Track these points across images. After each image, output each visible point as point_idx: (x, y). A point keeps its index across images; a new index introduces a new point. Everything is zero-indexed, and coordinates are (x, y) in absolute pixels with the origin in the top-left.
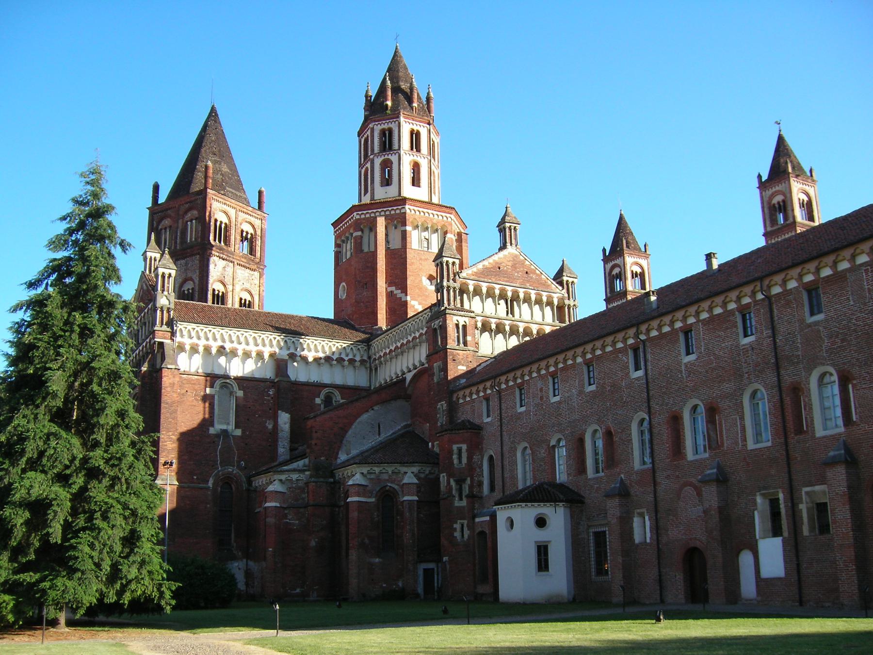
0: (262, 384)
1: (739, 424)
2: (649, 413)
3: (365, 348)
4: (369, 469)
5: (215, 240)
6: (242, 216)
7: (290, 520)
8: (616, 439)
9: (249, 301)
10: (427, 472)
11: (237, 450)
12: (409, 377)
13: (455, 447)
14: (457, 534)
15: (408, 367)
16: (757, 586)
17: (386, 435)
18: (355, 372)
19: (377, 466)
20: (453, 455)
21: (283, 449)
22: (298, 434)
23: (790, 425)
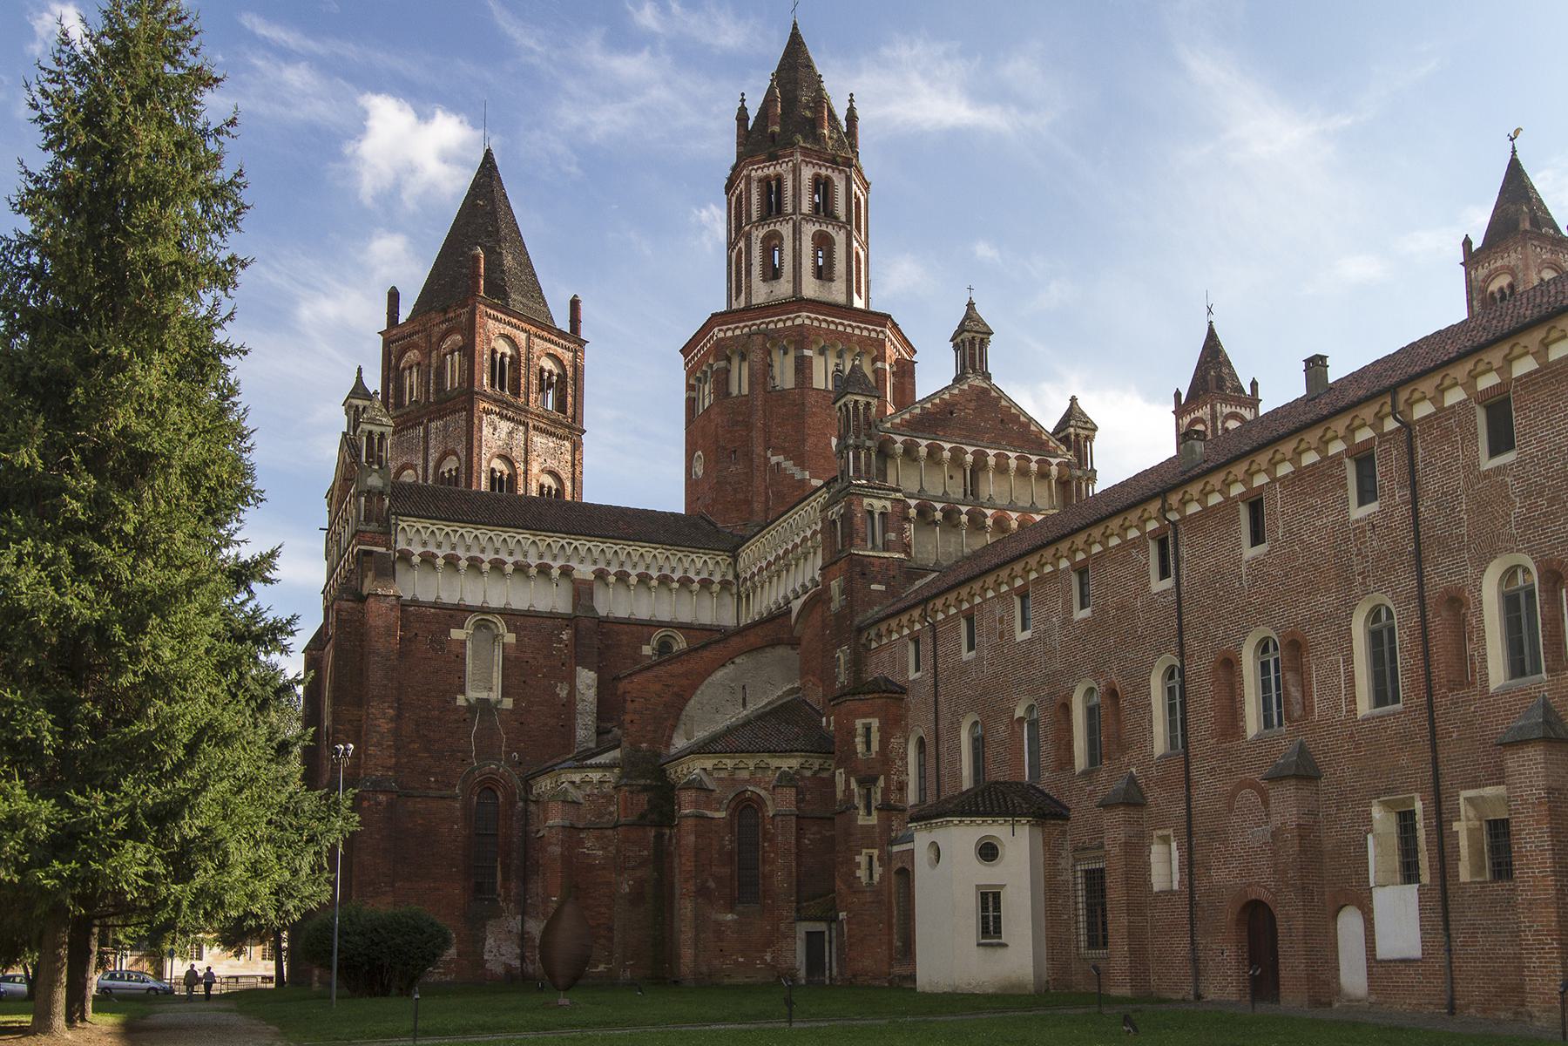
0: (549, 622)
1: (1342, 671)
2: (1182, 655)
3: (730, 560)
4: (716, 761)
5: (493, 386)
6: (539, 345)
10: (816, 767)
12: (796, 605)
14: (862, 873)
15: (794, 591)
16: (1370, 974)
17: (757, 704)
19: (729, 758)
21: (584, 731)
22: (608, 707)
23: (1440, 673)
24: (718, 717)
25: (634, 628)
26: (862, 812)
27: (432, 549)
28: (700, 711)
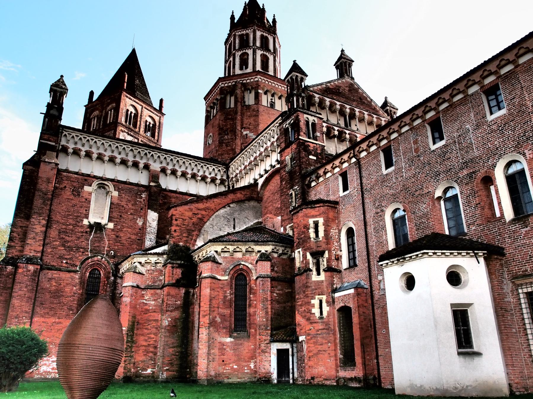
0: (136, 188)
3: (225, 170)
4: (223, 247)
5: (126, 122)
6: (146, 113)
7: (146, 300)
10: (280, 252)
11: (108, 241)
12: (261, 182)
13: (311, 221)
14: (316, 311)
18: (216, 188)
19: (231, 245)
20: (309, 229)
21: (149, 241)
25: (178, 195)
26: (315, 272)
27: (79, 146)
28: (211, 229)
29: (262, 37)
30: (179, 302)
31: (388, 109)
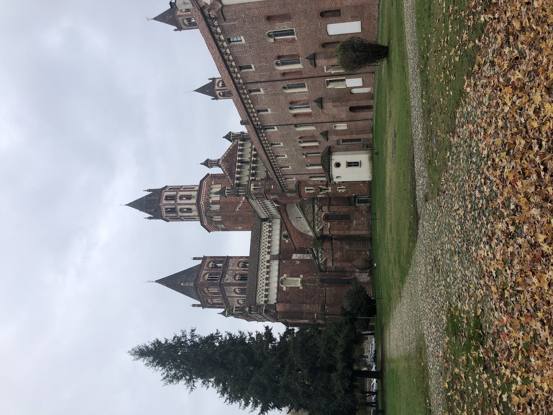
0: (281, 266)
8: (303, 136)
9: (243, 263)
10: (317, 201)
12: (276, 205)
13: (306, 192)
14: (343, 191)
17: (300, 214)
21: (308, 257)
22: (302, 251)
24: (304, 224)
25: (281, 245)
26: (328, 191)
27: (263, 295)
29: (166, 199)
30: (339, 242)
31: (232, 139)
